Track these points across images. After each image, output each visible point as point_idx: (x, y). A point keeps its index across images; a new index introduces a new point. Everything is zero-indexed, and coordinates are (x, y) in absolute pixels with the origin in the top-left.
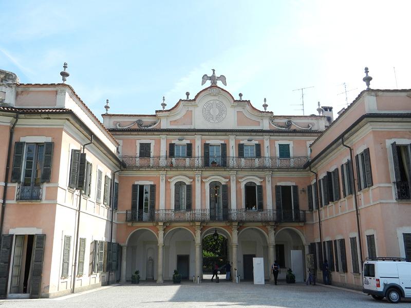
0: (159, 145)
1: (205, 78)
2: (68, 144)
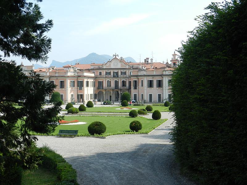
0: (104, 73)
1: (114, 55)
2: (85, 80)
